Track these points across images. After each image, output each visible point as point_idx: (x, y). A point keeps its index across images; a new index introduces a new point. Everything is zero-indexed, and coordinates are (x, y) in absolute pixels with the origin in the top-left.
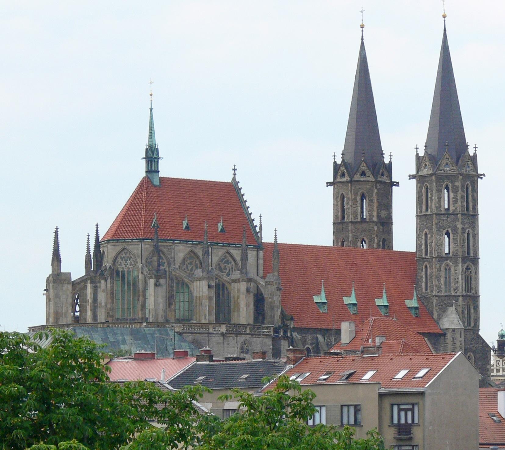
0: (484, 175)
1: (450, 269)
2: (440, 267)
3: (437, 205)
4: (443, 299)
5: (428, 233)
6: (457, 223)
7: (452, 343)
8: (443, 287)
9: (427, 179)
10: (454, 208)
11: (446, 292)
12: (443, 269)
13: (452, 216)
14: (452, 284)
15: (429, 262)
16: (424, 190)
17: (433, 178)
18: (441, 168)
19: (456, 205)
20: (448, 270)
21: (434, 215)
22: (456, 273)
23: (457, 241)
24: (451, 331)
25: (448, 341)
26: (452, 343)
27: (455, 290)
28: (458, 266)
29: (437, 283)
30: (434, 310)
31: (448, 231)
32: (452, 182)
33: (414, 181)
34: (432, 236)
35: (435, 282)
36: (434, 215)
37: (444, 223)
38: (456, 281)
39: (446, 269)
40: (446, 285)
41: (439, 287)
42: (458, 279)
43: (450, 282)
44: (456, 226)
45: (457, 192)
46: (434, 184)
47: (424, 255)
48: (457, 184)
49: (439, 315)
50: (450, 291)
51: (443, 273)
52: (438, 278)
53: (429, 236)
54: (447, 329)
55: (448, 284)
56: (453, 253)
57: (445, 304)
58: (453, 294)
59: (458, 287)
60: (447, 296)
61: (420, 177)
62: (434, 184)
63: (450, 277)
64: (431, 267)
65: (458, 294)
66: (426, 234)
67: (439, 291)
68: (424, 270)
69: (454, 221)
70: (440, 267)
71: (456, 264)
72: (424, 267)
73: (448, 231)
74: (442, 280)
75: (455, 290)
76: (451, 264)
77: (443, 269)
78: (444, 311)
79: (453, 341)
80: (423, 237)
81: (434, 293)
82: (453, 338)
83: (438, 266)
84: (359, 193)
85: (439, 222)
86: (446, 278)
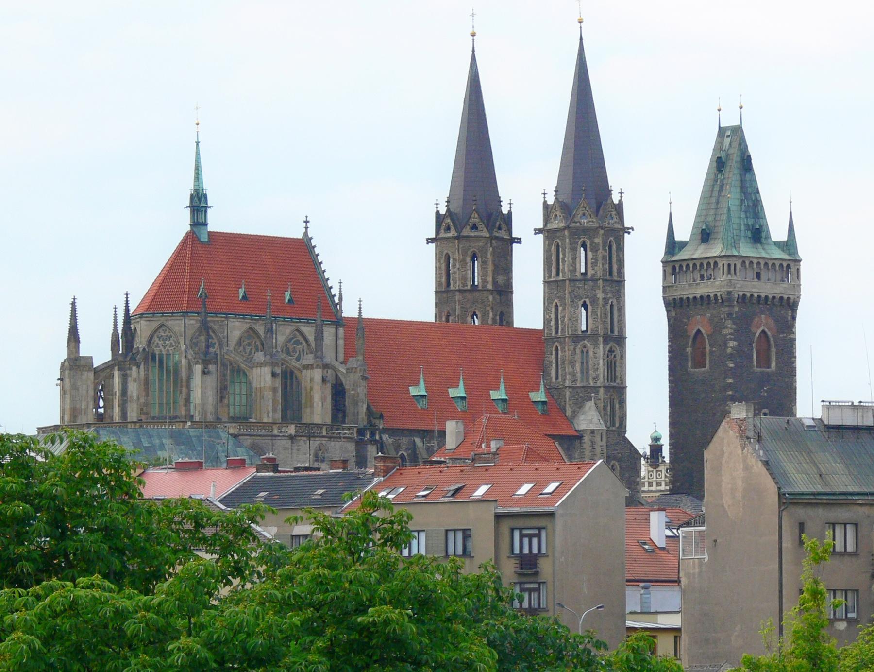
0: (632, 229)
1: (587, 352)
2: (575, 349)
4: (579, 391)
6: (597, 291)
8: (579, 375)
9: (558, 234)
10: (593, 272)
11: (582, 381)
12: (578, 351)
13: (591, 283)
14: (591, 372)
15: (560, 343)
16: (553, 248)
17: (566, 233)
18: (576, 220)
20: (585, 352)
25: (585, 446)
27: (594, 378)
29: (571, 370)
30: (567, 406)
31: (585, 302)
32: (590, 238)
34: (564, 309)
35: (569, 369)
37: (580, 291)
39: (582, 352)
40: (582, 373)
41: (573, 375)
43: (588, 369)
44: (595, 296)
46: (567, 240)
47: (553, 334)
48: (596, 240)
49: (573, 412)
50: (587, 380)
51: (578, 357)
52: (572, 363)
53: (560, 308)
54: (583, 431)
55: (585, 371)
56: (592, 330)
58: (592, 384)
59: (598, 376)
60: (583, 387)
61: (548, 231)
62: (567, 240)
63: (587, 362)
65: (598, 384)
66: (557, 306)
68: (554, 353)
70: (575, 349)
73: (585, 302)
75: (594, 378)
76: (589, 345)
77: (578, 351)
78: (580, 407)
79: (592, 446)
80: (553, 310)
81: (567, 383)
83: (572, 348)
84: (469, 253)
85: (573, 291)
86: (582, 363)
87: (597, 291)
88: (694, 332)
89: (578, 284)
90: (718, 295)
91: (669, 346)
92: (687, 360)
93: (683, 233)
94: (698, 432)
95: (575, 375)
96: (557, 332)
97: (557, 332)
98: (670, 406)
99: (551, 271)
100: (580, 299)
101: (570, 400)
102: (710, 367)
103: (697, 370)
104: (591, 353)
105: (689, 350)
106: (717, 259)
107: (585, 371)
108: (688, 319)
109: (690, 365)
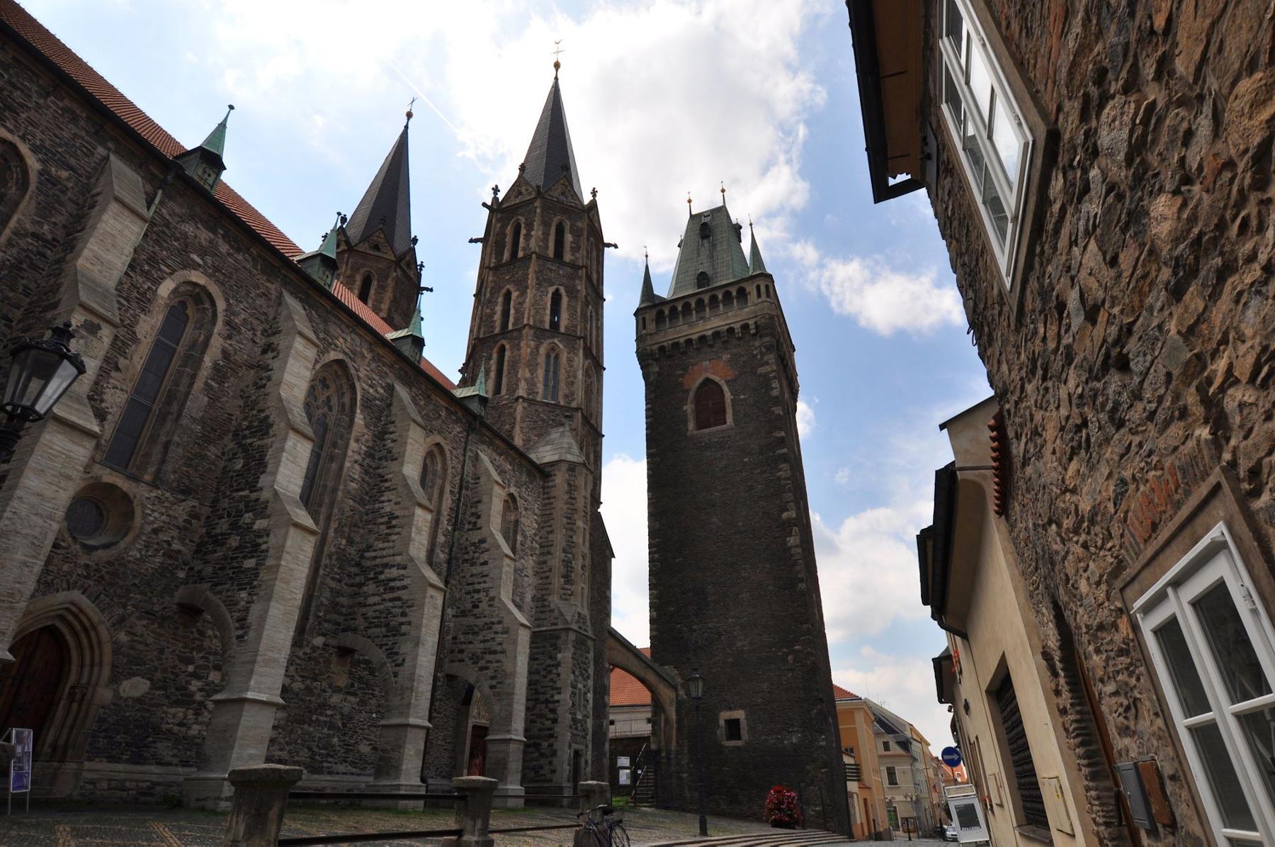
0: (616, 246)
1: (557, 357)
7: (566, 497)
9: (521, 211)
11: (545, 397)
12: (542, 350)
13: (569, 270)
14: (562, 385)
22: (571, 366)
24: (564, 467)
26: (566, 497)
27: (566, 396)
28: (576, 355)
29: (528, 375)
30: (517, 428)
31: (557, 290)
33: (480, 245)
35: (524, 373)
39: (548, 356)
40: (546, 385)
41: (531, 384)
42: (575, 377)
47: (497, 331)
48: (579, 224)
49: (527, 441)
50: (555, 396)
51: (541, 360)
52: (532, 366)
53: (515, 295)
54: (552, 464)
60: (547, 404)
63: (555, 373)
65: (574, 405)
66: (508, 294)
68: (495, 356)
69: (572, 277)
70: (537, 348)
71: (572, 350)
72: (495, 350)
73: (557, 290)
74: (540, 373)
75: (566, 396)
77: (542, 350)
78: (540, 436)
79: (569, 492)
80: (500, 300)
81: (521, 392)
82: (569, 485)
83: (532, 344)
84: (362, 271)
85: (541, 271)
86: (547, 371)
88: (698, 383)
89: (549, 265)
90: (751, 322)
93: (663, 290)
94: (715, 520)
98: (649, 490)
101: (523, 421)
102: (735, 420)
103: (706, 431)
104: (564, 357)
105: (689, 408)
106: (744, 285)
108: (685, 369)
109: (691, 426)
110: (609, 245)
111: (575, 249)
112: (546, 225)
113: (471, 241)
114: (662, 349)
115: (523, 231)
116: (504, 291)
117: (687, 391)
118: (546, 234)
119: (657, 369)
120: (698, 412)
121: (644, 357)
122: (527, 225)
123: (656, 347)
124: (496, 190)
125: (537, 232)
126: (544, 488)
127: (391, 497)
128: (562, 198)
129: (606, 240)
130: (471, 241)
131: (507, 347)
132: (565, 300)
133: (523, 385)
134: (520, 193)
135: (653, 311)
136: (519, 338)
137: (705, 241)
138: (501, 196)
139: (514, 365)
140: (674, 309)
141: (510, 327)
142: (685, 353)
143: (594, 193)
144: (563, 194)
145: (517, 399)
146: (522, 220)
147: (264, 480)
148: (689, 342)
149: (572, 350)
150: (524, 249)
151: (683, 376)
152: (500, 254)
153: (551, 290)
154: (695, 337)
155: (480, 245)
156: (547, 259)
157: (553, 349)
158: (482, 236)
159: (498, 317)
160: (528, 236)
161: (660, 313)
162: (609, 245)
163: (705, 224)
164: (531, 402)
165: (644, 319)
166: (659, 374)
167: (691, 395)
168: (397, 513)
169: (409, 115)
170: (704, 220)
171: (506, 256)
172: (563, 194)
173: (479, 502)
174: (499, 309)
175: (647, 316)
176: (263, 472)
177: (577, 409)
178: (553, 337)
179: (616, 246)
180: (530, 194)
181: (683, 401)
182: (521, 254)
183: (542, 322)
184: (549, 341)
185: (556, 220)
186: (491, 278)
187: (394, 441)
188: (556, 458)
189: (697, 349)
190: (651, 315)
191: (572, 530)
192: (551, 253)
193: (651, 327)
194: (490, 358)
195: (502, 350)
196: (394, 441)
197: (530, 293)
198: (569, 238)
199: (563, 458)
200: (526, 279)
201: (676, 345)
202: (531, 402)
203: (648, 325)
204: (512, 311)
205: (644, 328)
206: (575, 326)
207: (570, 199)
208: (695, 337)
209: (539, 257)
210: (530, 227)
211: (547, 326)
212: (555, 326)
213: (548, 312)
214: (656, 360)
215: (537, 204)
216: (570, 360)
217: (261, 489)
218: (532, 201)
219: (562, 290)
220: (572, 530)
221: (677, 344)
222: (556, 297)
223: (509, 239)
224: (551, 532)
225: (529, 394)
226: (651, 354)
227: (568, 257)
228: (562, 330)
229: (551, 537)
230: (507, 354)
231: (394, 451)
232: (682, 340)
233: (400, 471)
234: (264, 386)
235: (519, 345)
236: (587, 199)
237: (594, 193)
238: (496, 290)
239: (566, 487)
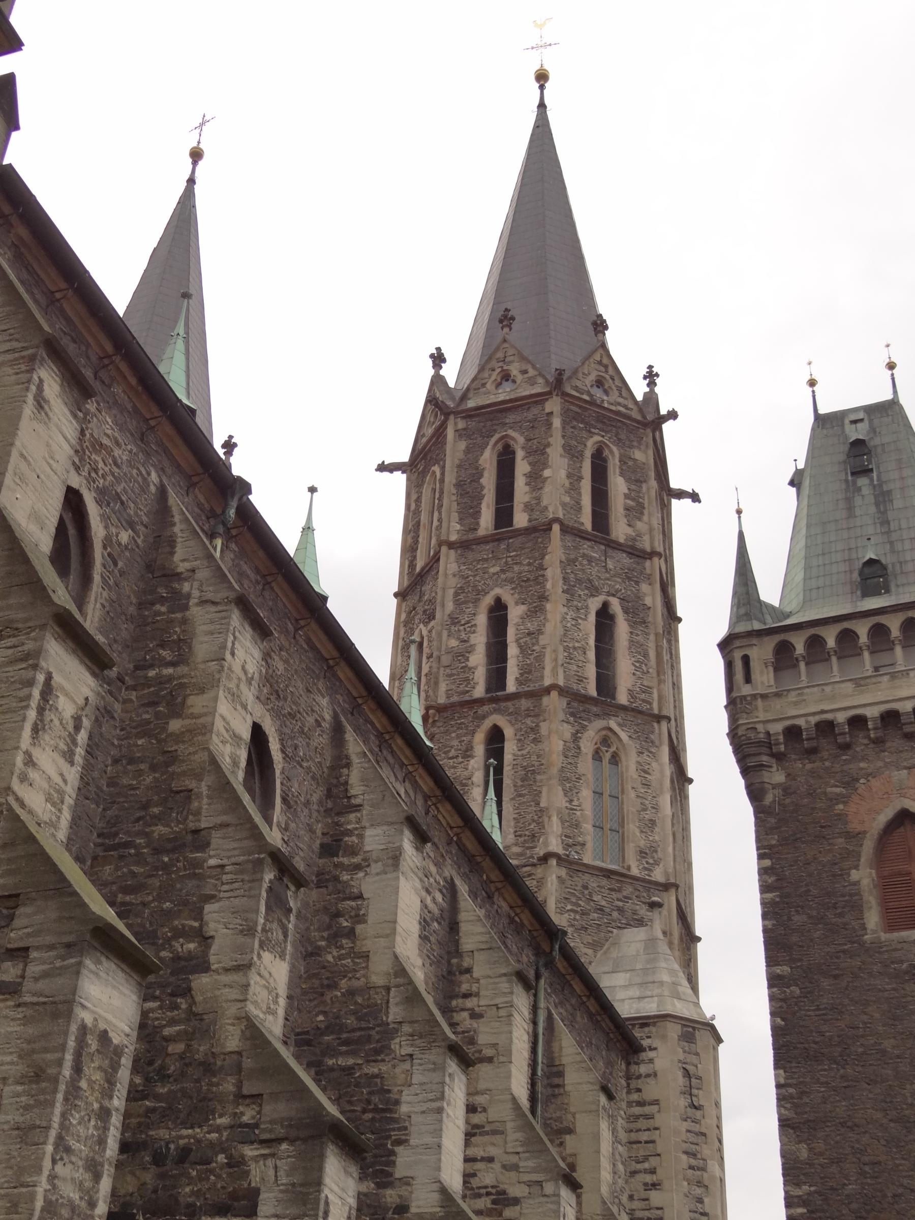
0: (695, 497)
1: (615, 760)
2: (576, 738)
3: (567, 499)
4: (593, 883)
5: (508, 598)
8: (588, 827)
9: (511, 418)
12: (587, 745)
13: (626, 560)
14: (632, 828)
15: (515, 716)
16: (488, 459)
17: (554, 405)
18: (579, 384)
19: (639, 525)
20: (607, 752)
21: (556, 527)
22: (647, 785)
23: (646, 655)
24: (673, 1031)
25: (651, 1090)
32: (619, 442)
33: (400, 479)
36: (556, 527)
37: (594, 571)
38: (648, 815)
39: (597, 756)
41: (572, 824)
42: (656, 808)
44: (639, 597)
45: (639, 482)
47: (479, 691)
48: (638, 455)
51: (586, 765)
52: (570, 782)
53: (515, 613)
54: (645, 1022)
56: (630, 692)
57: (601, 909)
58: (635, 871)
61: (469, 415)
62: (557, 422)
64: (532, 735)
65: (658, 875)
67: (572, 842)
68: (479, 749)
70: (576, 738)
71: (647, 745)
72: (480, 738)
74: (586, 795)
75: (642, 854)
79: (689, 1091)
80: (482, 620)
81: (555, 845)
82: (687, 1074)
83: (567, 731)
85: (571, 562)
87: (644, 587)
89: (586, 547)
91: (763, 872)
92: (856, 906)
95: (577, 826)
96: (497, 677)
97: (497, 677)
99: (477, 514)
100: (594, 591)
105: (864, 876)
107: (612, 827)
108: (850, 783)
109: (873, 919)
110: (681, 494)
111: (635, 511)
112: (572, 453)
113: (382, 468)
114: (792, 733)
115: (522, 467)
116: (488, 600)
117: (857, 837)
118: (574, 477)
119: (778, 777)
120: (888, 885)
121: (749, 750)
122: (530, 453)
123: (777, 728)
124: (438, 359)
125: (557, 468)
126: (628, 1078)
127: (492, 1151)
128: (598, 393)
129: (674, 484)
130: (382, 468)
131: (508, 732)
132: (622, 629)
133: (555, 826)
134: (506, 377)
135: (758, 642)
136: (537, 713)
137: (862, 481)
138: (450, 373)
139: (530, 774)
140: (815, 643)
141: (511, 686)
142: (847, 747)
143: (651, 376)
144: (599, 383)
145: (545, 859)
146: (518, 440)
147: (405, 1162)
148: (857, 722)
149: (647, 745)
150: (528, 508)
151: (844, 799)
152: (470, 512)
153: (595, 604)
154: (872, 713)
155: (400, 479)
156: (580, 534)
157: (605, 741)
158: (405, 457)
159: (478, 659)
160: (535, 479)
161: (783, 651)
162: (681, 494)
163: (858, 444)
164: (573, 866)
165: (746, 660)
166: (787, 790)
167: (868, 847)
168: (515, 1191)
169: (196, 155)
170: (855, 433)
171: (486, 520)
172: (599, 383)
173: (570, 1131)
174: (480, 639)
175: (754, 653)
176: (399, 1142)
177: (666, 887)
178: (606, 715)
179: (695, 497)
180: (532, 382)
181: (853, 856)
182: (521, 519)
183: (581, 679)
184: (600, 724)
185: (591, 443)
186: (453, 567)
187: (475, 1015)
188: (650, 1008)
189: (878, 742)
190: (761, 653)
191: (700, 1183)
192: (586, 520)
193: (764, 678)
194: (467, 753)
195: (496, 737)
196: (475, 1015)
197: (556, 610)
198: (618, 486)
199: (669, 1010)
200: (539, 579)
201: (826, 728)
202: (573, 866)
203: (756, 675)
204: (512, 651)
205: (748, 680)
206: (647, 690)
207: (614, 396)
208: (872, 713)
209: (565, 530)
210: (538, 456)
211: (593, 691)
212: (605, 683)
213: (591, 655)
214: (779, 757)
215: (554, 405)
216: (644, 771)
217: (406, 1181)
218: (539, 399)
219: (616, 606)
220: (700, 1183)
221: (831, 724)
222: (604, 617)
223: (489, 481)
224: (655, 1186)
225: (567, 846)
226: (768, 743)
227: (620, 530)
228: (622, 698)
229: (656, 1197)
230: (510, 748)
231: (482, 1039)
232: (841, 717)
233: (509, 1089)
234: (351, 934)
235: (535, 729)
236: (639, 389)
237: (651, 376)
238: (467, 595)
239: (681, 1080)
